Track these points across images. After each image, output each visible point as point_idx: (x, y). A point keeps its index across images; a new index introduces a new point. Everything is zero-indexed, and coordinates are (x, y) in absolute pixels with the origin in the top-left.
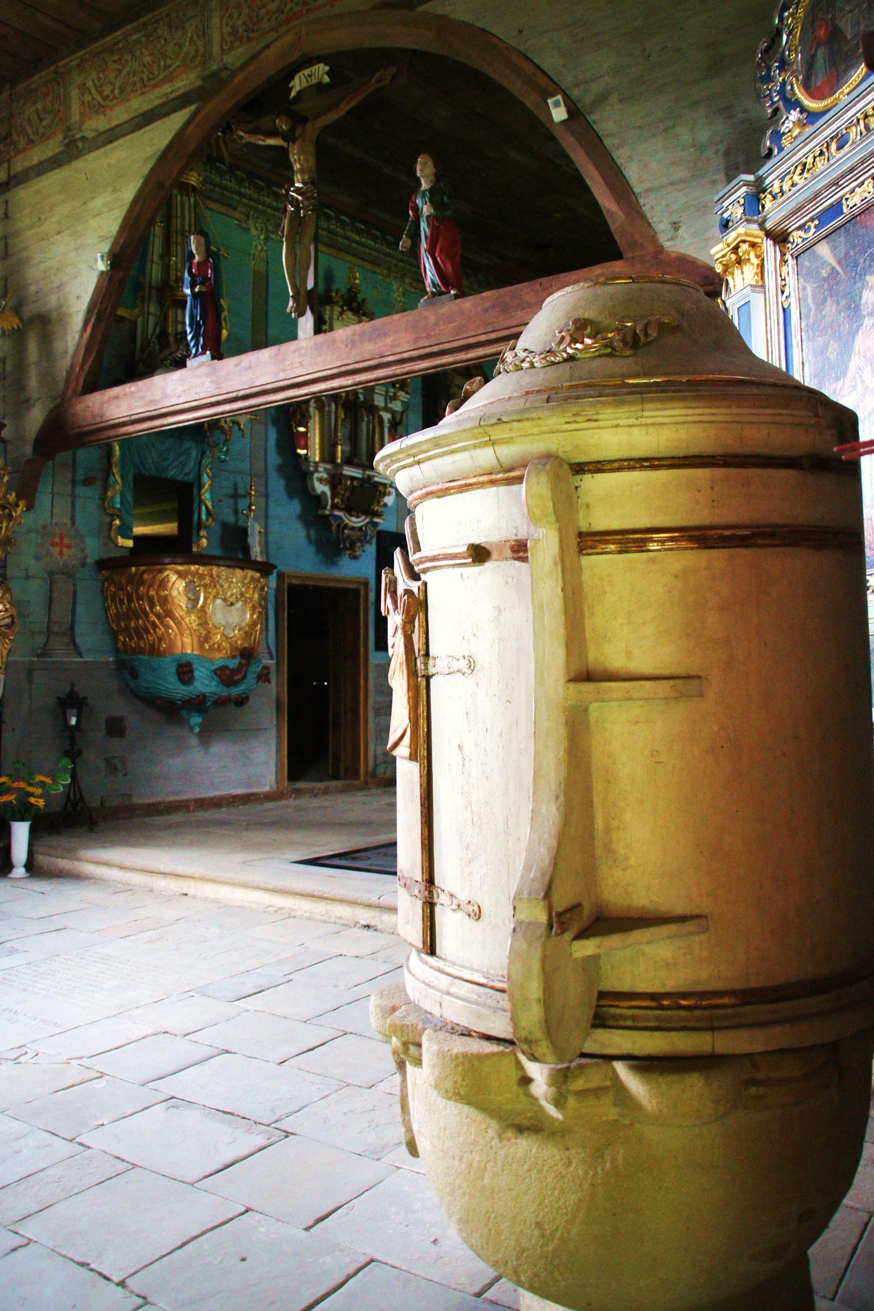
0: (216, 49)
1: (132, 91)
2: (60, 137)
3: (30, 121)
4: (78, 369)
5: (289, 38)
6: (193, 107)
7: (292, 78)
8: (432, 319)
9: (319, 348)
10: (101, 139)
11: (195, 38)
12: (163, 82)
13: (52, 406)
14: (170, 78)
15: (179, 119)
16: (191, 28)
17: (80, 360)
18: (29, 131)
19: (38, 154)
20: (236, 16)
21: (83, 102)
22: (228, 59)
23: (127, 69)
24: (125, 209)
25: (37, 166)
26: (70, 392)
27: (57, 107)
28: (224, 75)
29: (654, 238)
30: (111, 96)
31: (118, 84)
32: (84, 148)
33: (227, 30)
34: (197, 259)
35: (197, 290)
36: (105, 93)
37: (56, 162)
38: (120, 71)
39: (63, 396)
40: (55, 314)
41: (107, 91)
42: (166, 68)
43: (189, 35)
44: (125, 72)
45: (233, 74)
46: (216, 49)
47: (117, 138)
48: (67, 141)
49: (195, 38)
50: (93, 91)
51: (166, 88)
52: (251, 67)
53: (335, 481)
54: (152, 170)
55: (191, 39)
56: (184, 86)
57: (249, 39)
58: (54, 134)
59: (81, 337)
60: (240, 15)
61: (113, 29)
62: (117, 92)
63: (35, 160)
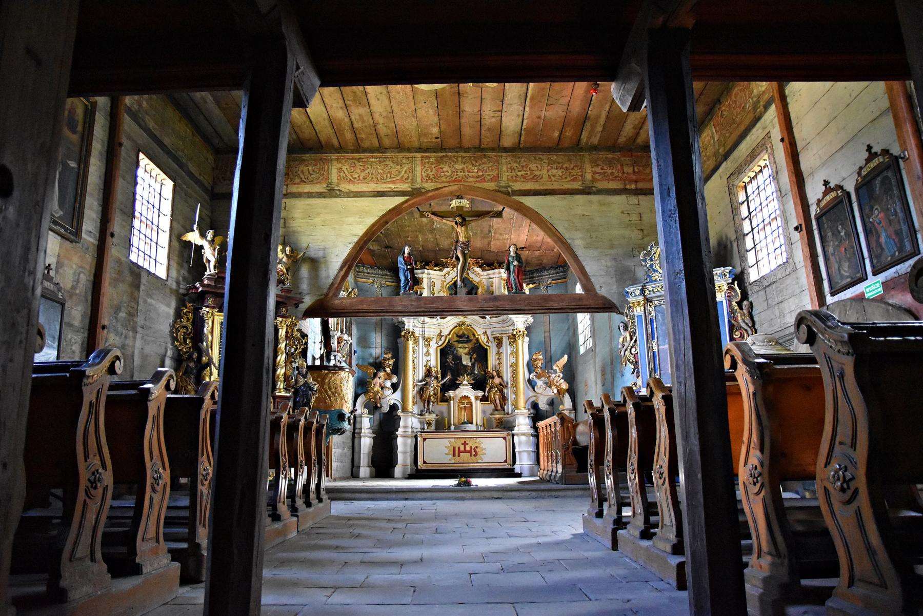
0: (419, 180)
1: (371, 180)
2: (325, 185)
3: (302, 172)
4: (336, 285)
5: (455, 188)
6: (407, 198)
7: (451, 201)
8: (519, 299)
9: (470, 300)
10: (352, 195)
11: (408, 171)
12: (389, 182)
13: (318, 298)
14: (393, 182)
15: (399, 200)
16: (405, 167)
17: (338, 282)
18: (302, 176)
19: (307, 188)
20: (429, 171)
21: (339, 175)
22: (425, 185)
23: (368, 170)
24: (367, 227)
25: (305, 193)
26: (331, 294)
27: (322, 172)
28: (423, 191)
29: (595, 289)
30: (358, 179)
31: (363, 175)
32: (340, 195)
33: (424, 175)
34: (406, 255)
35: (409, 267)
36: (354, 176)
37: (320, 195)
38: (364, 171)
39: (326, 295)
40: (322, 260)
41: (356, 176)
42: (390, 178)
43: (405, 169)
44: (367, 172)
45: (427, 192)
46: (419, 180)
47: (361, 197)
48: (329, 188)
49: (408, 171)
50: (346, 172)
51: (391, 185)
52: (437, 192)
53: (340, 340)
54: (383, 216)
55: (405, 172)
56: (401, 188)
57: (436, 182)
58: (320, 183)
59: (339, 272)
60: (431, 171)
61: (358, 152)
62: (361, 178)
63: (306, 191)
